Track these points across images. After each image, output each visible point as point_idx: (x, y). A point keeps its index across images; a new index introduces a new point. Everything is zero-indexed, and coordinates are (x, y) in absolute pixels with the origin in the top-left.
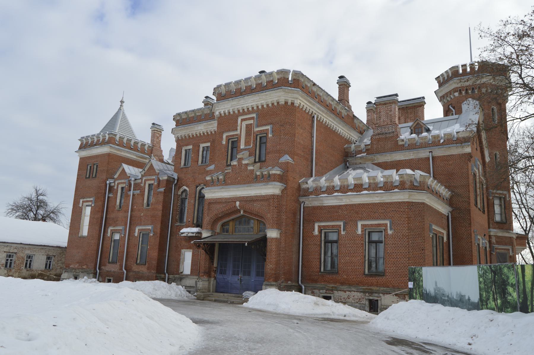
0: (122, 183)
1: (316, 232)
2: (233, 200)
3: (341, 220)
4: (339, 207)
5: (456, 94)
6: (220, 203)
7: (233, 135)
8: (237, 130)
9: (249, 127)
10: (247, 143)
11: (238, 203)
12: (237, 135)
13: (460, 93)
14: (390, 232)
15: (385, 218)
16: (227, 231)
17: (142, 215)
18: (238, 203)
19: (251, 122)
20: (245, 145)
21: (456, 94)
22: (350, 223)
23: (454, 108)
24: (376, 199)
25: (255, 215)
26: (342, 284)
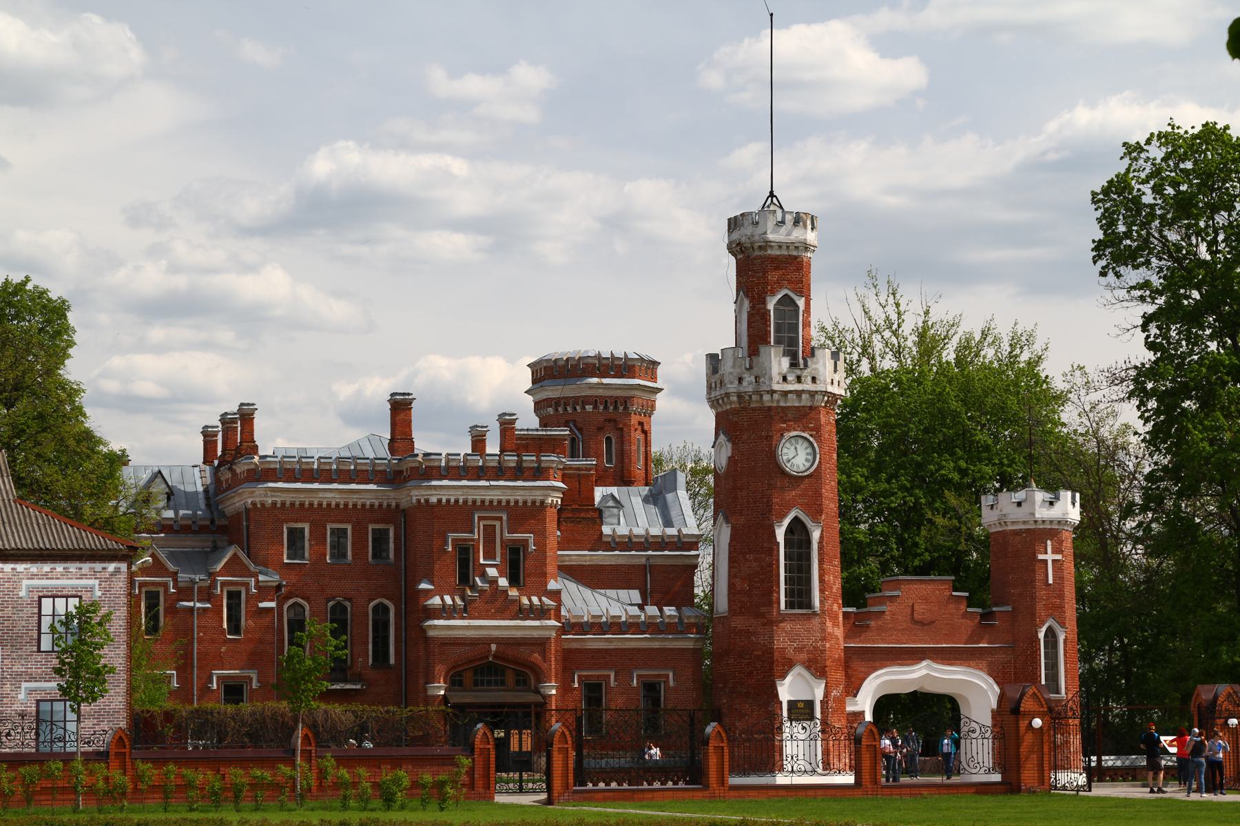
0: (153, 584)
1: (576, 685)
2: (487, 641)
3: (610, 669)
4: (607, 651)
5: (589, 408)
6: (459, 644)
7: (465, 540)
8: (472, 532)
9: (489, 533)
10: (489, 555)
11: (494, 647)
12: (473, 540)
13: (595, 407)
14: (671, 683)
15: (666, 668)
16: (460, 683)
17: (223, 649)
18: (494, 647)
19: (498, 524)
20: (485, 559)
21: (589, 408)
22: (623, 673)
23: (580, 430)
24: (656, 645)
25: (515, 663)
26: (613, 749)
